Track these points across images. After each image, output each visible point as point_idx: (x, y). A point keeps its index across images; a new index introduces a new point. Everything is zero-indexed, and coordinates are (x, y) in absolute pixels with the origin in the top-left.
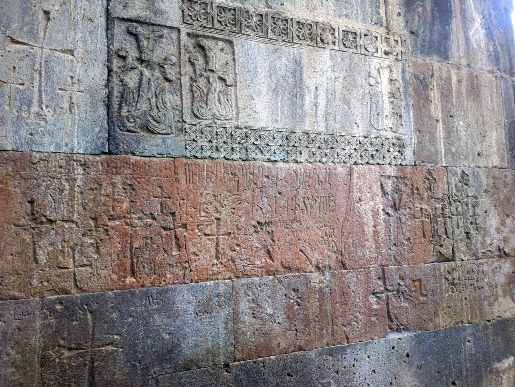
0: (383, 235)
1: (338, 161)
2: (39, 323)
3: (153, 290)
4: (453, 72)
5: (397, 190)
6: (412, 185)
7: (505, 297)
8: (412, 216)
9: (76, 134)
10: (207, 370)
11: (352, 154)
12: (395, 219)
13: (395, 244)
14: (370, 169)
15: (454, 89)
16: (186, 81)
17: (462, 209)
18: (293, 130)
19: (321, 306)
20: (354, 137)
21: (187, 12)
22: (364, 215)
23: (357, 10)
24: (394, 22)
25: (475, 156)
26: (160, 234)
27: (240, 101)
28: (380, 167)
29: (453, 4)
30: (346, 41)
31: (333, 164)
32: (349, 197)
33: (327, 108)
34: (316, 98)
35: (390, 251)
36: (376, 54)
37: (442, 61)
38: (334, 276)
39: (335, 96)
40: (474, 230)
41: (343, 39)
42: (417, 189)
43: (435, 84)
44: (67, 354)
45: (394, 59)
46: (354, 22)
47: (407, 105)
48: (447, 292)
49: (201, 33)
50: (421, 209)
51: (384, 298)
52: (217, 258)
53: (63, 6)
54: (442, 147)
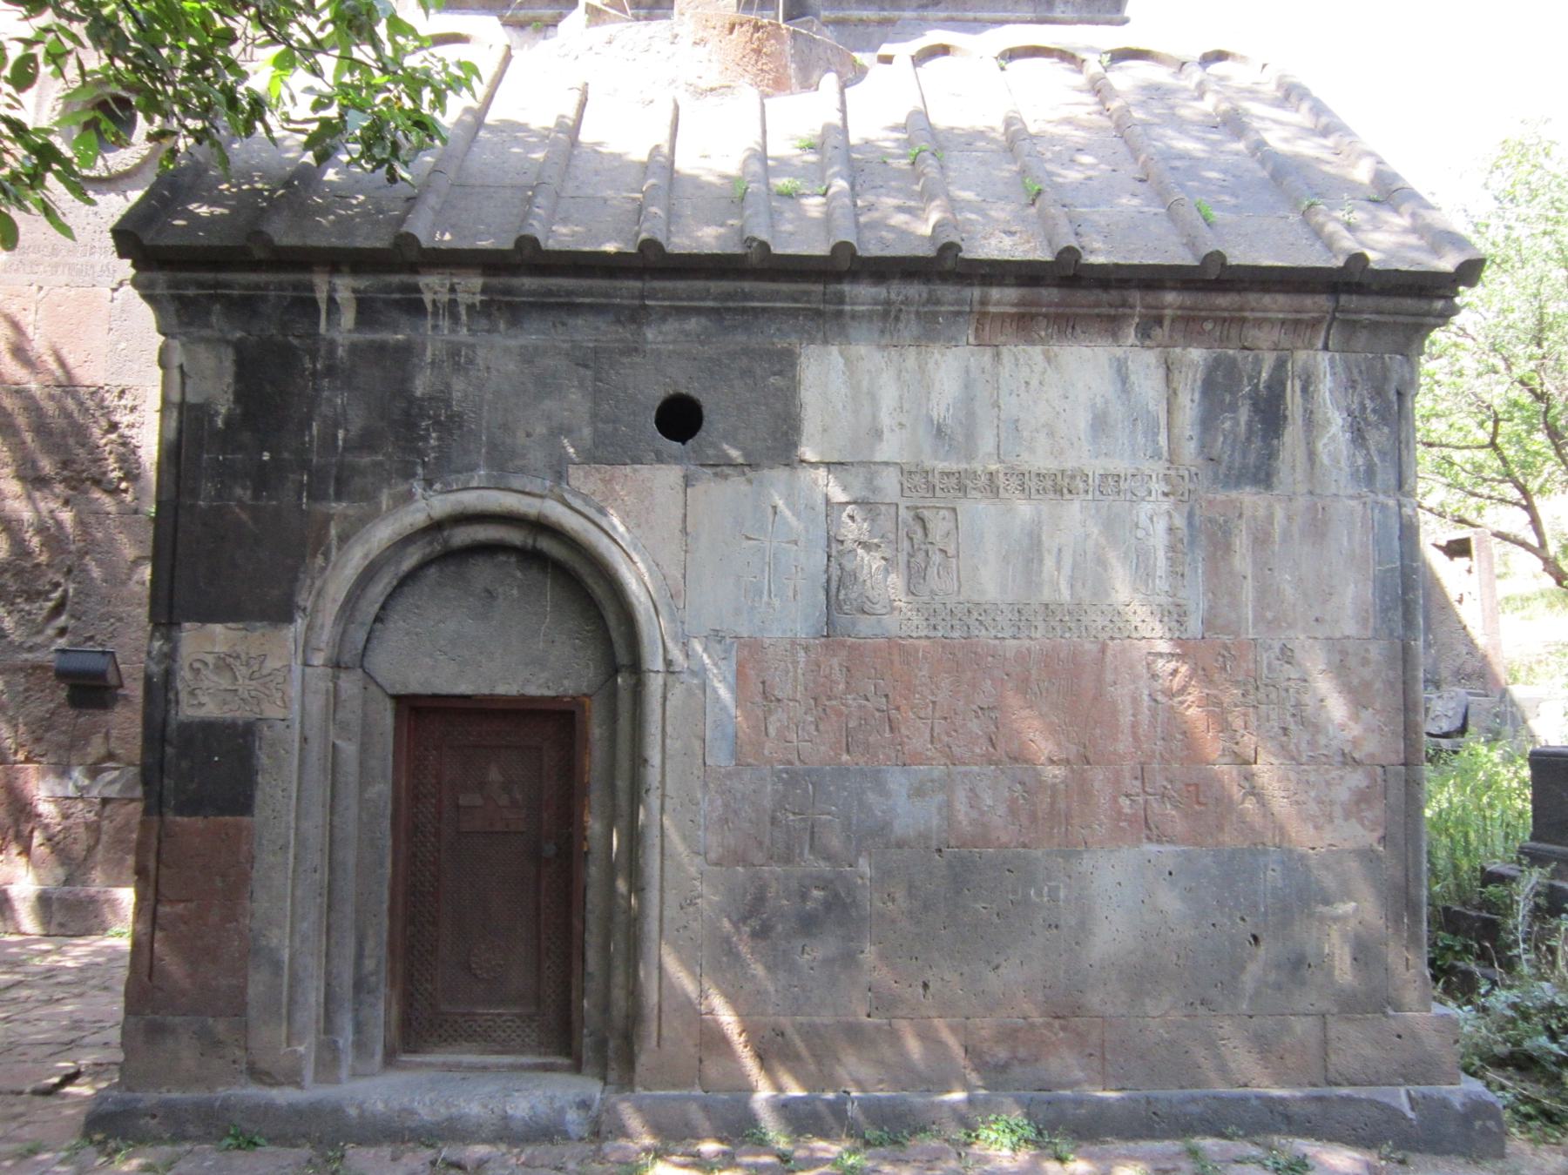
2: (769, 788)
7: (1346, 818)
19: (1052, 804)
21: (906, 484)
27: (962, 573)
32: (1099, 679)
38: (1072, 771)
43: (1244, 527)
44: (791, 817)
52: (932, 742)
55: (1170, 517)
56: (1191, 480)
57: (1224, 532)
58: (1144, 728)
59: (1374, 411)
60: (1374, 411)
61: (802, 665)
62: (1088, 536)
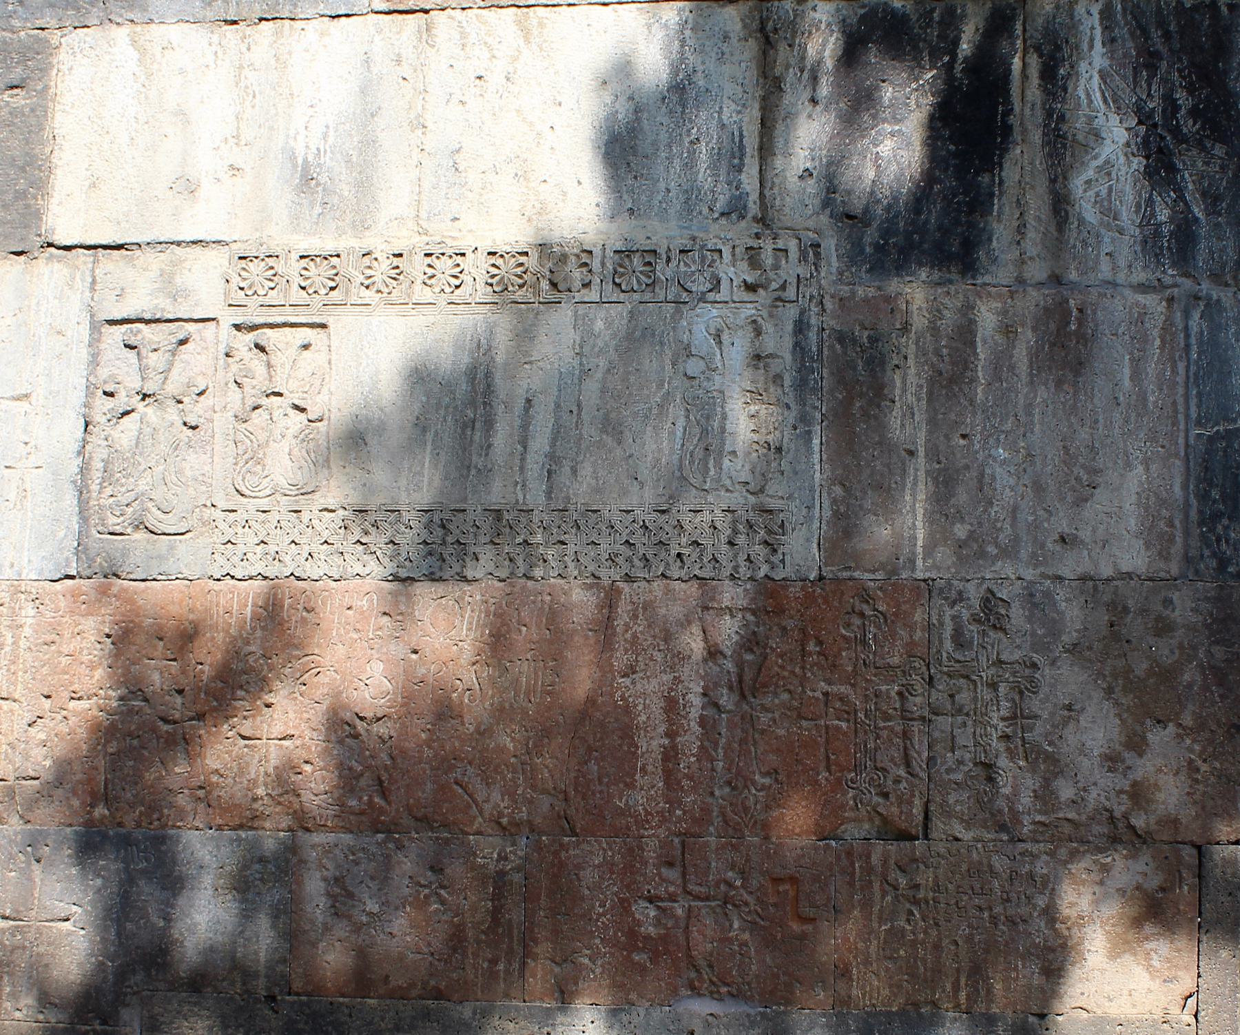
0: (693, 759)
1: (576, 573)
3: (138, 834)
4: (983, 309)
5: (751, 642)
6: (803, 631)
8: (795, 714)
9: (26, 545)
10: (232, 998)
11: (616, 555)
12: (737, 719)
13: (729, 783)
14: (668, 591)
15: (982, 356)
16: (223, 423)
17: (975, 699)
18: (458, 506)
19: (496, 913)
20: (628, 512)
21: (235, 280)
22: (640, 707)
23: (668, 191)
24: (788, 199)
25: (1043, 546)
26: (154, 730)
28: (700, 587)
29: (1017, 108)
30: (622, 275)
31: (562, 581)
33: (553, 444)
34: (525, 427)
35: (710, 800)
36: (711, 296)
37: (951, 282)
38: (539, 847)
39: (579, 414)
40: (1012, 754)
41: (616, 272)
42: (820, 643)
43: (911, 350)
45: (769, 301)
46: (655, 223)
47: (804, 419)
48: (892, 920)
49: (261, 320)
50: (826, 694)
51: (680, 912)
53: (19, 315)
54: (919, 524)
55: (758, 332)
56: (803, 257)
57: (869, 362)
58: (688, 761)
59: (1194, 113)
60: (1194, 113)
61: (27, 631)
62: (586, 372)
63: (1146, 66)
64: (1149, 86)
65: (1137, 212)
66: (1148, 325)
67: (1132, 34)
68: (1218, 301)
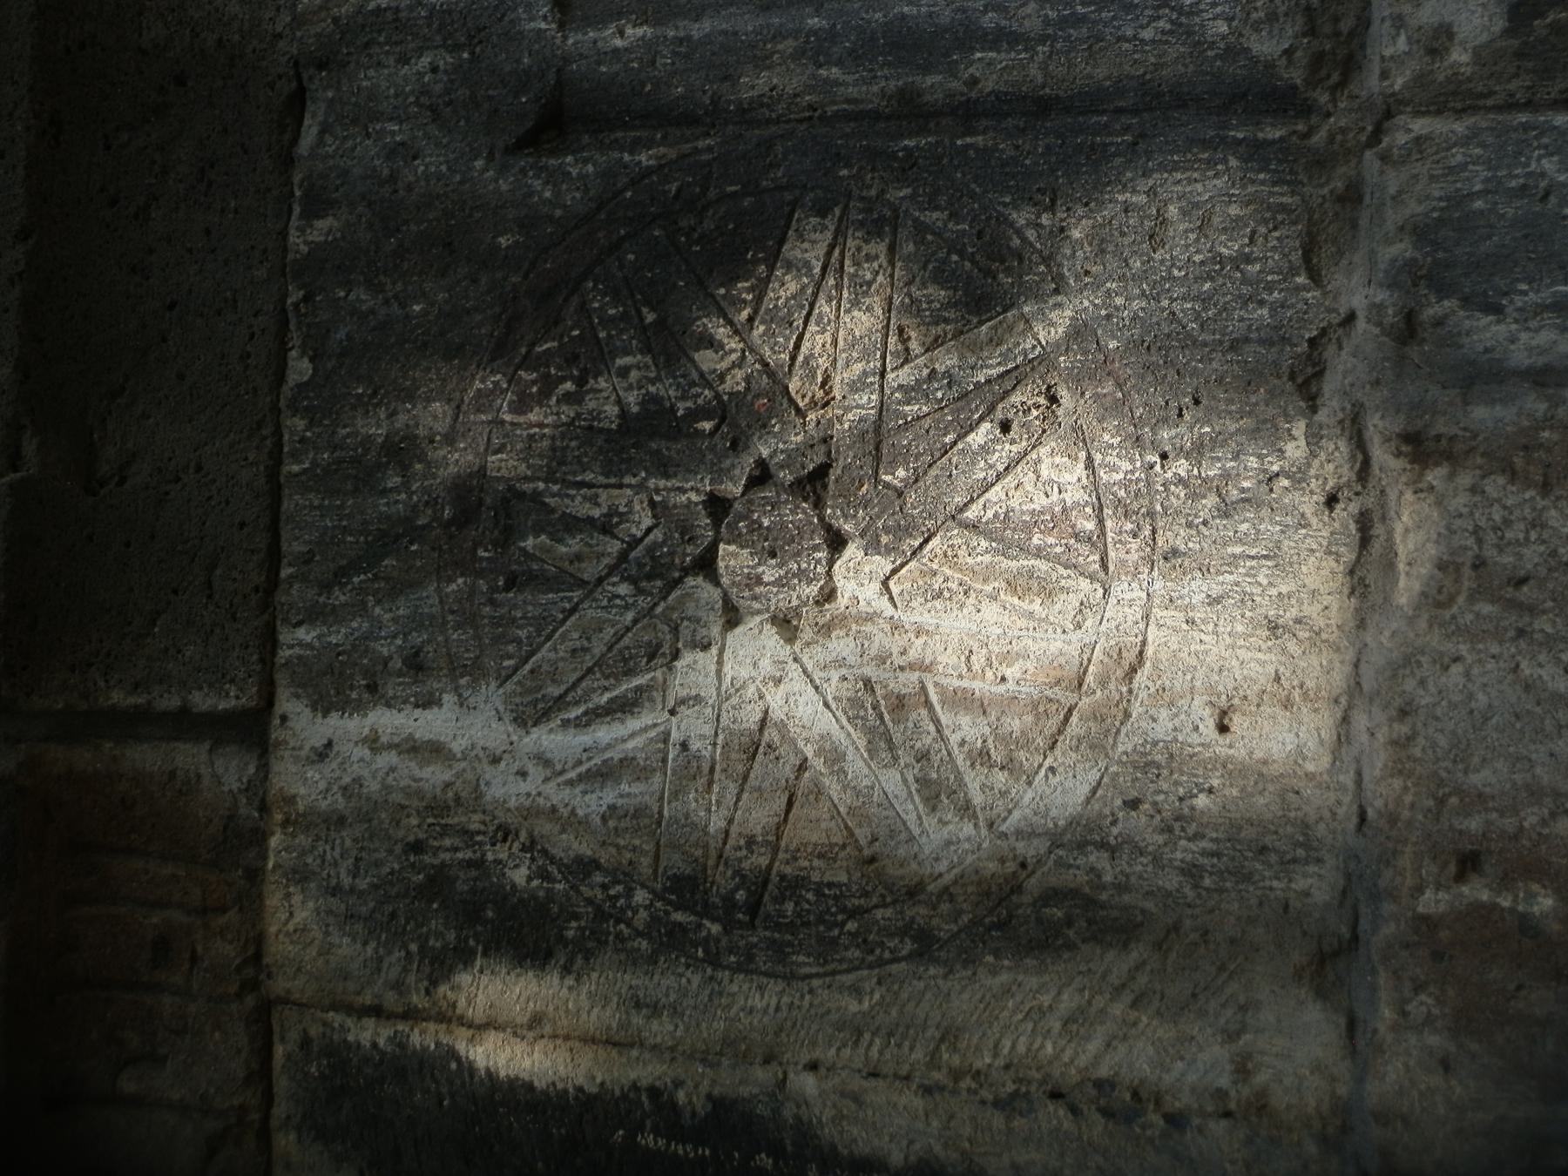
63: (507, 536)
64: (572, 524)
65: (1048, 592)
66: (1532, 556)
67: (396, 589)
68: (1421, 232)
